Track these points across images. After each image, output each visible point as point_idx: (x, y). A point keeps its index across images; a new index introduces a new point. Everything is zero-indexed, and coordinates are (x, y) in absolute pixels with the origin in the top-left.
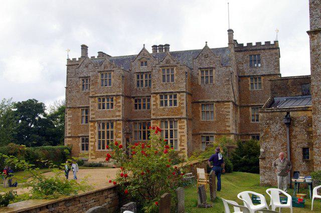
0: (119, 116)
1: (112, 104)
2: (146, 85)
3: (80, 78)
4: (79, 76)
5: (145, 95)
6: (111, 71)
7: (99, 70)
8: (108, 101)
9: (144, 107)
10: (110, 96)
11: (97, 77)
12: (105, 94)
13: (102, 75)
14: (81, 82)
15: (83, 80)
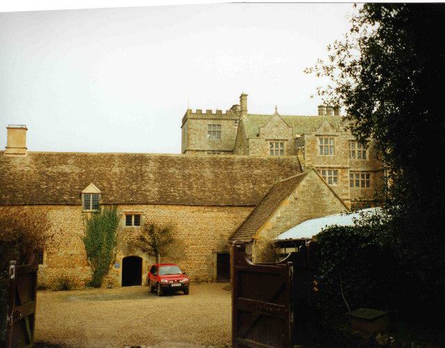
0: (347, 194)
1: (335, 178)
2: (359, 157)
3: (266, 140)
4: (266, 138)
5: (360, 169)
6: (335, 136)
7: (318, 133)
8: (330, 174)
9: (358, 185)
10: (334, 168)
11: (314, 142)
12: (327, 166)
13: (321, 140)
14: (269, 146)
15: (271, 144)
